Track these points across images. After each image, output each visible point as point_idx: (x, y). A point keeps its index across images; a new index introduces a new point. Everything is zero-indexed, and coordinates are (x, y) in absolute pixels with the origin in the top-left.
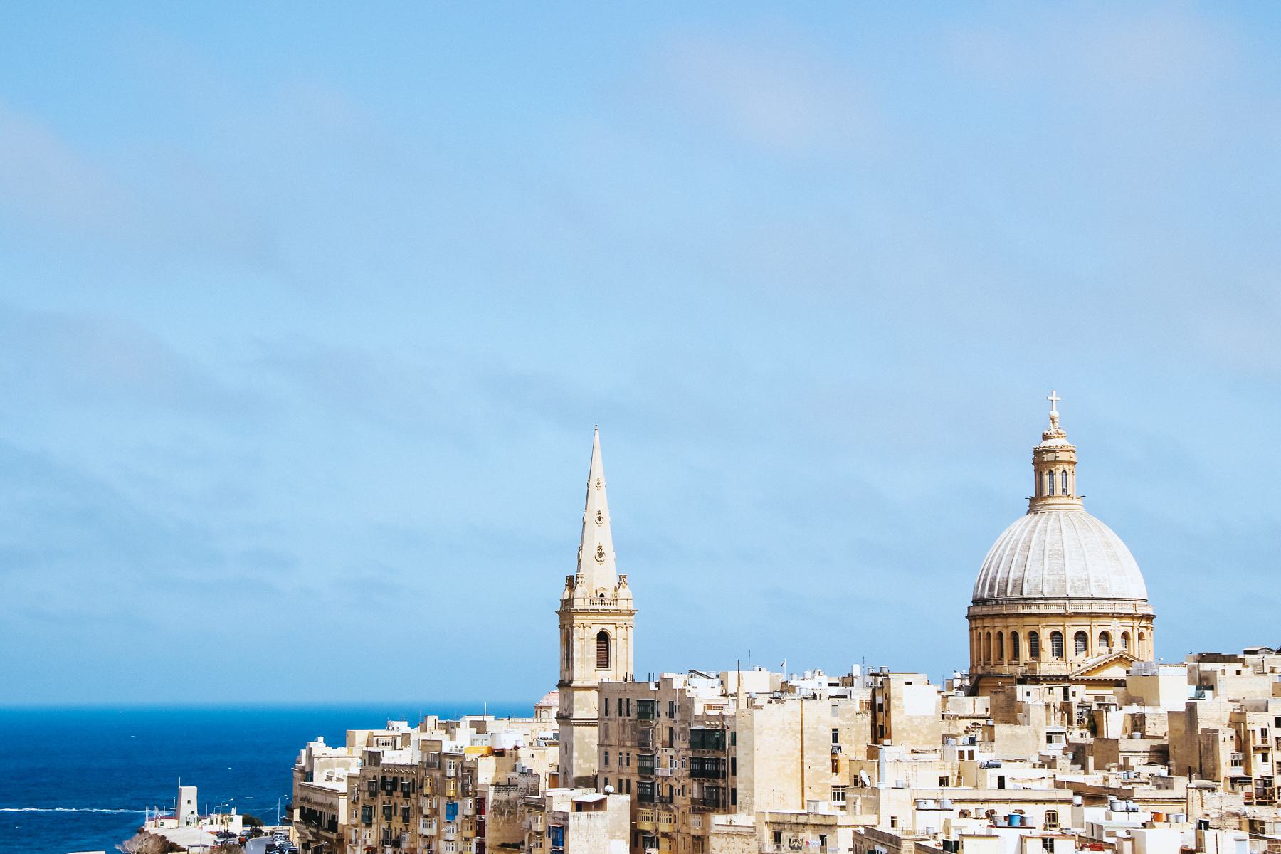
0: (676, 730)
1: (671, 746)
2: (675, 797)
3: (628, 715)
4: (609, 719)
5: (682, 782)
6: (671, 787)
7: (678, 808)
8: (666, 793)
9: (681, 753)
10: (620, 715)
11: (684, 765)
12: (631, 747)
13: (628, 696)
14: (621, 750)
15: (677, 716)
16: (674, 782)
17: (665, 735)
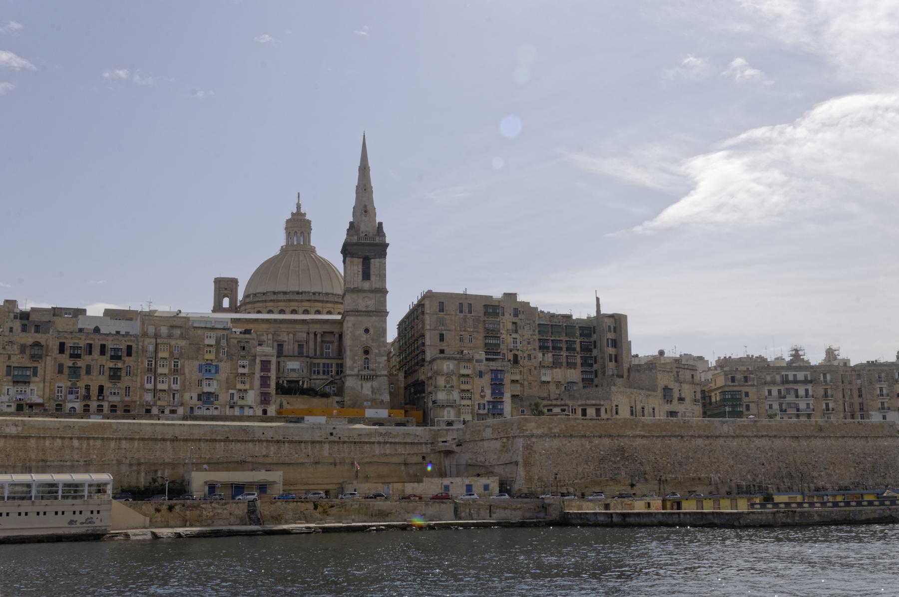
0: (519, 323)
1: (516, 332)
2: (521, 362)
3: (470, 312)
4: (445, 315)
5: (527, 352)
6: (515, 356)
7: (523, 367)
8: (511, 357)
9: (526, 337)
10: (461, 312)
11: (529, 343)
12: (473, 332)
13: (470, 302)
14: (462, 333)
15: (520, 316)
16: (520, 353)
17: (510, 326)
